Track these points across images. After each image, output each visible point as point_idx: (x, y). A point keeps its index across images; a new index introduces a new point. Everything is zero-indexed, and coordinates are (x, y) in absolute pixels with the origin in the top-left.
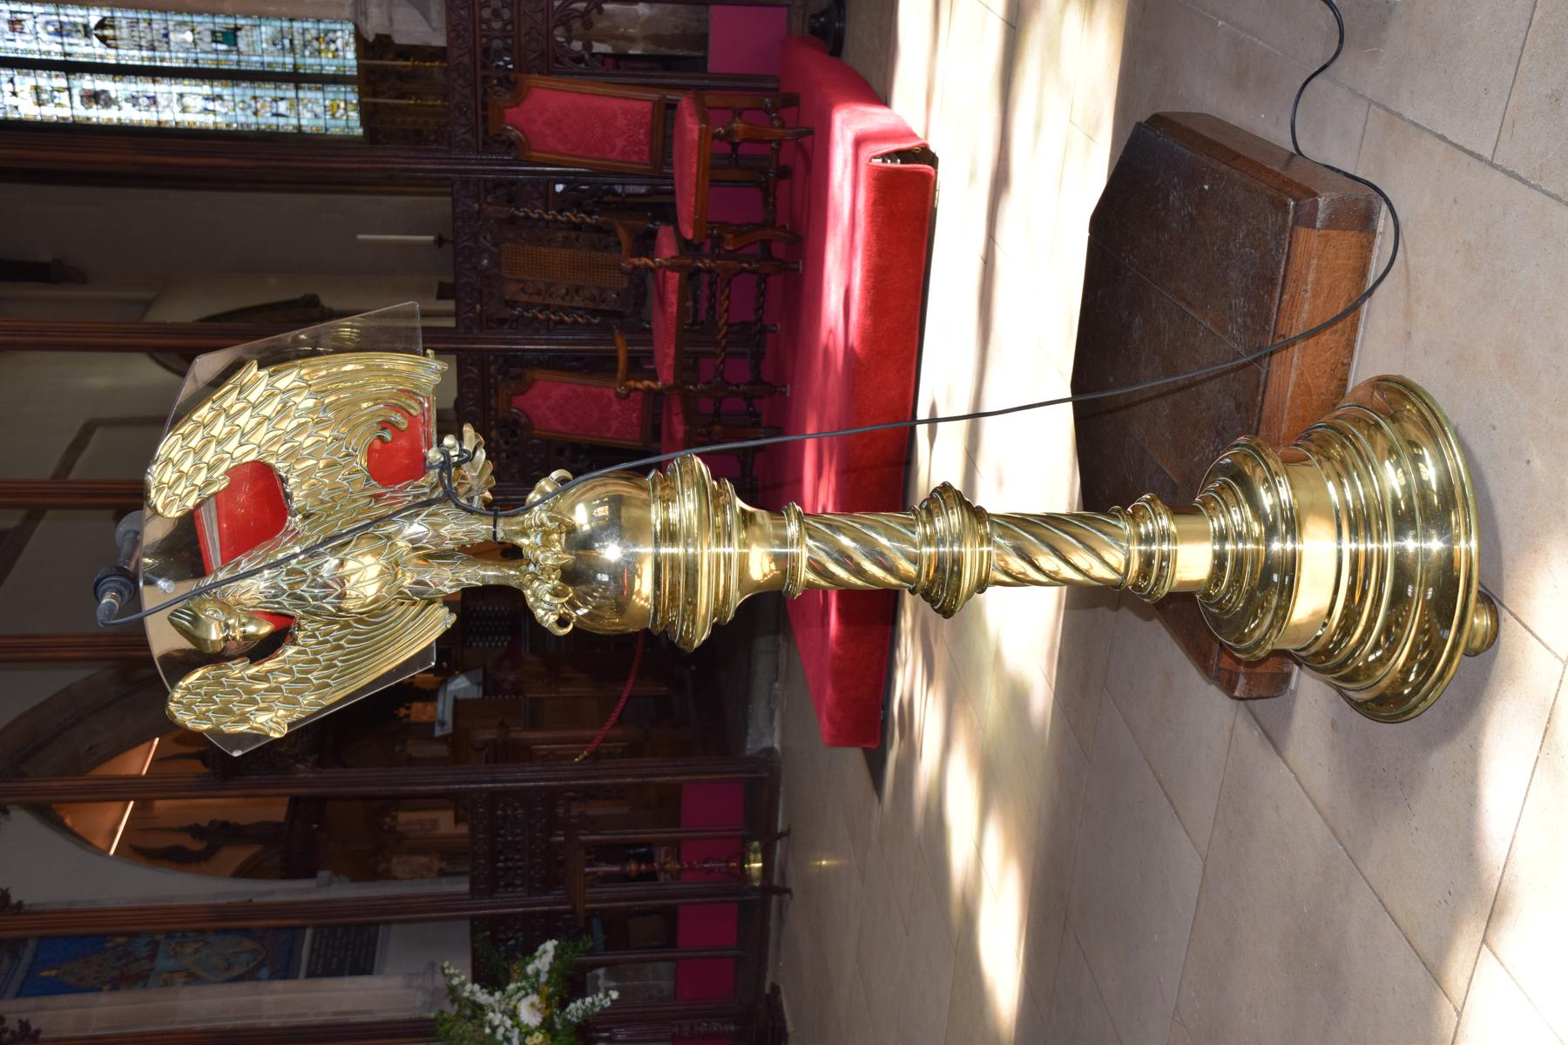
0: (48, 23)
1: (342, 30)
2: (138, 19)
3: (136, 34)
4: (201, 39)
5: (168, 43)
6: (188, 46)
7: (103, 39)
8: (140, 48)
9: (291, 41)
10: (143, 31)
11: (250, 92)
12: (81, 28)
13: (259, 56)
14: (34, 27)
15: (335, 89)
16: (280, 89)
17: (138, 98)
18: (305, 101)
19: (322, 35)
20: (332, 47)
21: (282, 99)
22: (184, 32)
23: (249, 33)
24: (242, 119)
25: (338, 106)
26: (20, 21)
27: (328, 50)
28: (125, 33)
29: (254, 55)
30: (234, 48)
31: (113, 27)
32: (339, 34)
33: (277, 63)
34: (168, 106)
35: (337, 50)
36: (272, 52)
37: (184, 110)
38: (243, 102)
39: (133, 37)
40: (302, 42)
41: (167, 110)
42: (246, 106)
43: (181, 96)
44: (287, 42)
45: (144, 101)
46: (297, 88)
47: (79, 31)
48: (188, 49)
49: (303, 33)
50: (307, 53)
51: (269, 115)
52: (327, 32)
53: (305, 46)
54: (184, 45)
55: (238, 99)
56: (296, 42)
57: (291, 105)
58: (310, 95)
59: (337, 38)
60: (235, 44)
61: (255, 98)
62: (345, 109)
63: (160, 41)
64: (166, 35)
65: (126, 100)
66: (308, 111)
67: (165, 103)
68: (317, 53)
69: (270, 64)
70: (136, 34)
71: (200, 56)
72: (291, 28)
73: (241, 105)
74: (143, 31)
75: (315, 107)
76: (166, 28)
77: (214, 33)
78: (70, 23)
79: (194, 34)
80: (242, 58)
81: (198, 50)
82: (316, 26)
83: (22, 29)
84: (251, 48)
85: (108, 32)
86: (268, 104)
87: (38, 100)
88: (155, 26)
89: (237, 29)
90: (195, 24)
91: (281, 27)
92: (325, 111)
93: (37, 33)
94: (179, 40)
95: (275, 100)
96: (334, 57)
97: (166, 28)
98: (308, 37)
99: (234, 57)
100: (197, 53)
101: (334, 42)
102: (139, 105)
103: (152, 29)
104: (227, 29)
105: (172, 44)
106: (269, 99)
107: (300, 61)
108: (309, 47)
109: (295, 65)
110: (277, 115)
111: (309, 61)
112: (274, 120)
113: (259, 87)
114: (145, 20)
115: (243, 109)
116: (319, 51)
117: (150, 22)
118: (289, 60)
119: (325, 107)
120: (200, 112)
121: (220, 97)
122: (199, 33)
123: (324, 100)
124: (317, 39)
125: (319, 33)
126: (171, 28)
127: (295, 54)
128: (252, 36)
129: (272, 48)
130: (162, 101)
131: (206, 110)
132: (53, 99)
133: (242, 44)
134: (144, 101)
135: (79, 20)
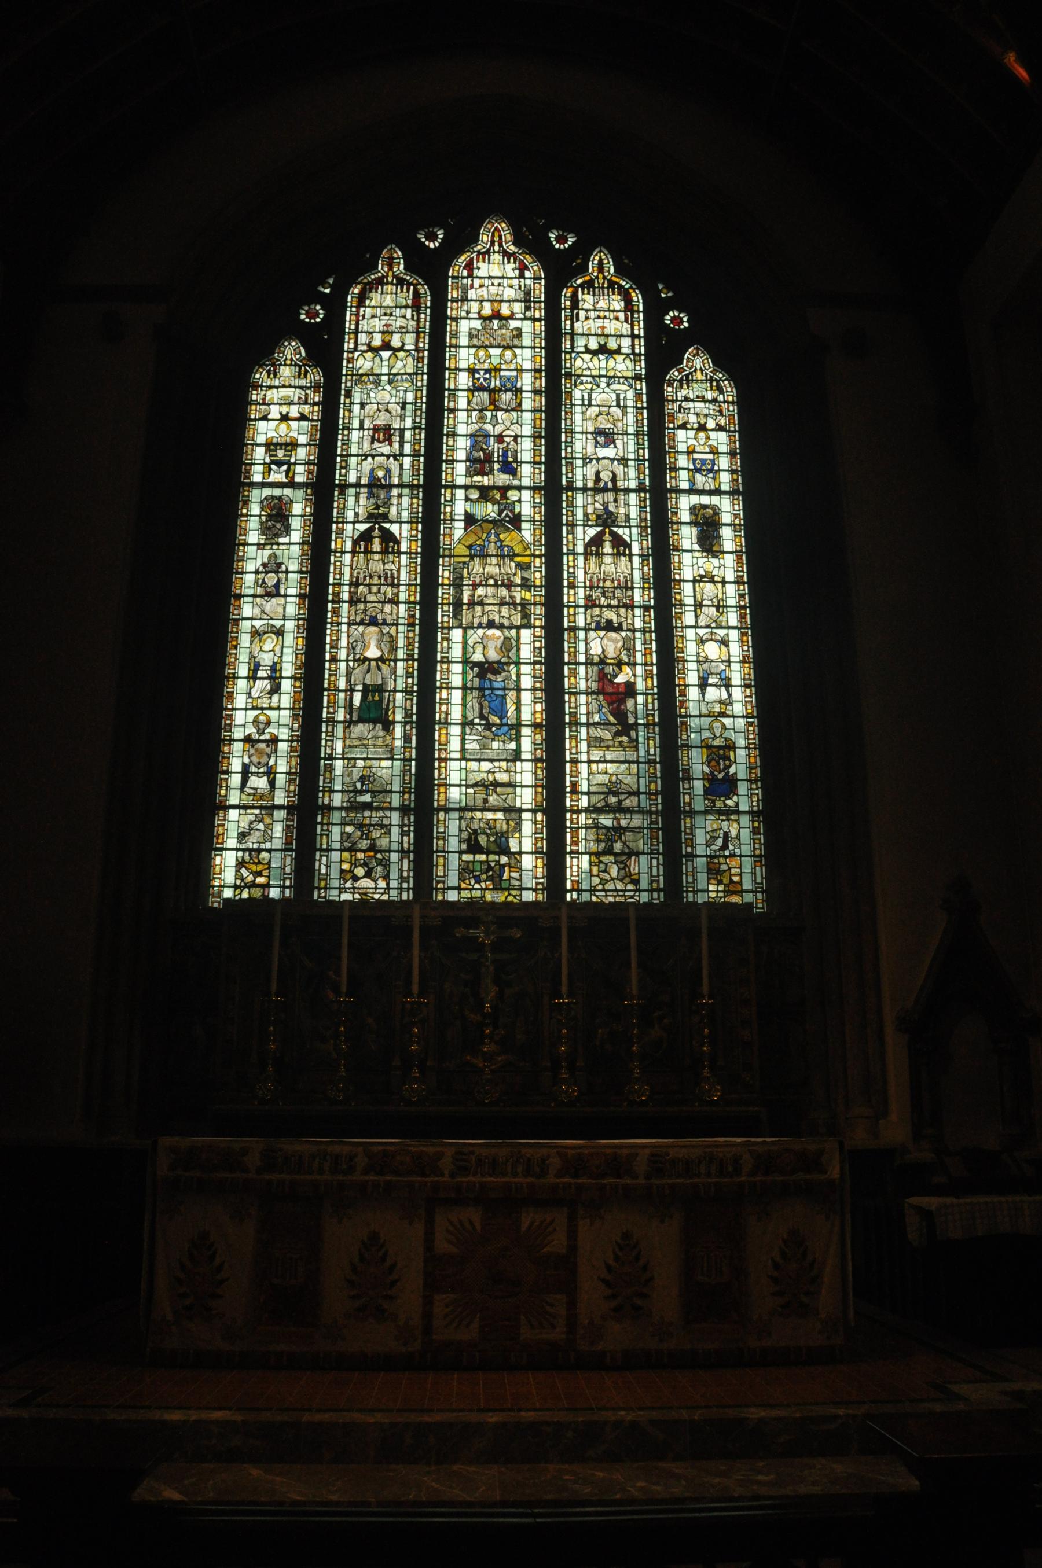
0: (388, 471)
1: (388, 888)
2: (398, 585)
3: (376, 580)
4: (369, 671)
5: (362, 623)
6: (358, 650)
7: (366, 537)
8: (355, 584)
9: (368, 806)
10: (379, 591)
11: (284, 734)
12: (382, 510)
13: (344, 753)
14: (382, 455)
15: (288, 870)
16: (290, 782)
17: (277, 572)
18: (267, 820)
19: (379, 856)
20: (360, 872)
21: (272, 783)
22: (379, 647)
23: (380, 742)
24: (239, 717)
25: (259, 874)
26: (389, 440)
27: (354, 864)
28: (376, 565)
29: (344, 747)
30: (355, 718)
31: (385, 551)
32: (382, 884)
33: (332, 780)
34: (263, 612)
35: (356, 878)
36: (350, 775)
37: (256, 634)
38: (268, 723)
39: (371, 577)
40: (367, 821)
41: (257, 611)
42: (262, 726)
43: (280, 633)
44: (367, 798)
45: (271, 579)
46: (289, 808)
47: (378, 507)
48: (354, 649)
49: (382, 826)
50: (349, 829)
51: (246, 760)
52: (385, 864)
53: (360, 826)
54: (359, 643)
55: (273, 714)
56: (367, 813)
57: (262, 797)
58: (278, 830)
59: (375, 881)
60: (361, 720)
61: (274, 740)
62: (253, 885)
63: (365, 611)
64: (374, 622)
65: (274, 556)
66: (251, 823)
67: (268, 607)
68: (348, 845)
69: (330, 769)
70: (376, 580)
71: (343, 666)
72: (391, 809)
73: (262, 718)
74: (379, 591)
75: (257, 833)
76: (385, 623)
77: (380, 689)
78: (389, 498)
79: (376, 660)
80: (340, 727)
81: (351, 664)
82: (395, 846)
83: (379, 441)
84: (356, 743)
85: (376, 545)
86: (264, 760)
87: (276, 445)
88: (387, 608)
89: (388, 726)
90: (392, 663)
91: (391, 792)
92: (250, 850)
93: (373, 456)
94: (367, 639)
95: (271, 774)
96: (342, 871)
97: (385, 623)
98: (376, 834)
99: (341, 716)
100: (347, 661)
101: (368, 875)
102: (267, 573)
103: (384, 602)
104: (387, 709)
105: (361, 628)
106: (272, 762)
107: (336, 817)
108: (359, 833)
109: (330, 808)
110: (245, 773)
111: (336, 832)
112: (236, 765)
113: (292, 749)
114: (397, 595)
115: (256, 721)
116: (352, 850)
117: (394, 601)
118: (337, 800)
119: (259, 851)
120: (252, 657)
121: (276, 689)
122: (379, 669)
123: (269, 851)
124: (372, 848)
125: (381, 852)
126: (385, 630)
127: (347, 809)
128: (375, 746)
129: (356, 774)
130: (272, 605)
131: (255, 667)
132: (279, 464)
133: (360, 729)
134: (271, 579)
135: (394, 510)
